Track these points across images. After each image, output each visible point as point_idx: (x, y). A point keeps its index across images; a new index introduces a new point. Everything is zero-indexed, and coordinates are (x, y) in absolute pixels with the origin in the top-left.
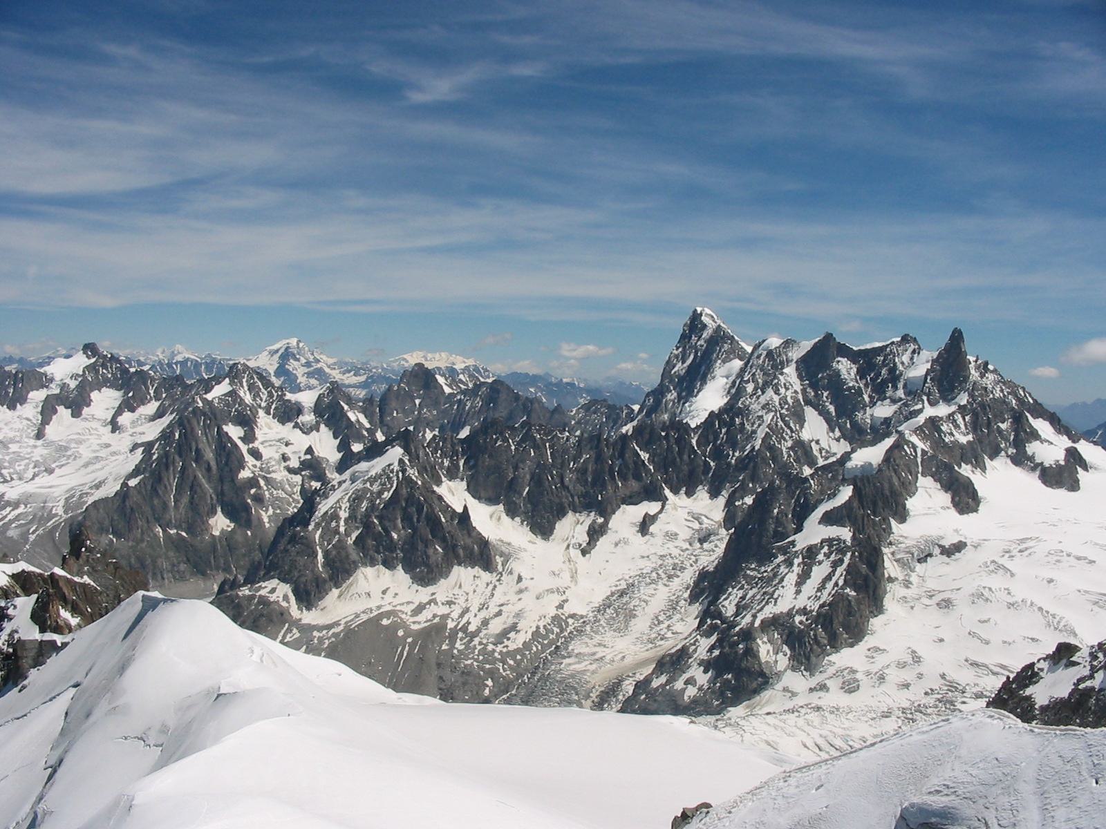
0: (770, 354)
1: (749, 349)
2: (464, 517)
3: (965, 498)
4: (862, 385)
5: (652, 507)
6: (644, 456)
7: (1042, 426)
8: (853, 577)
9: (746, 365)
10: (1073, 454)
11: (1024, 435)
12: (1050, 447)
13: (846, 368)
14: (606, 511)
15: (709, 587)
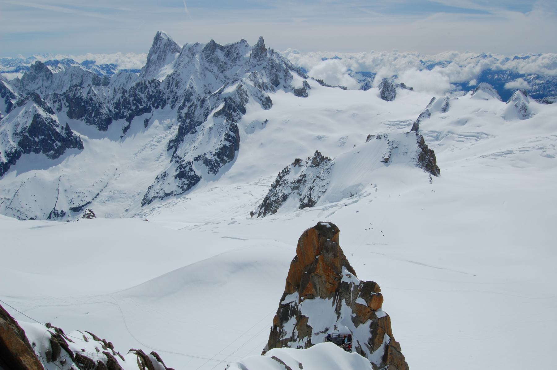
0: (190, 49)
1: (182, 47)
2: (68, 129)
3: (267, 103)
4: (227, 61)
5: (146, 115)
6: (142, 95)
7: (294, 74)
8: (228, 138)
9: (181, 54)
10: (306, 84)
11: (287, 77)
12: (298, 82)
13: (219, 54)
14: (130, 119)
15: (174, 145)
